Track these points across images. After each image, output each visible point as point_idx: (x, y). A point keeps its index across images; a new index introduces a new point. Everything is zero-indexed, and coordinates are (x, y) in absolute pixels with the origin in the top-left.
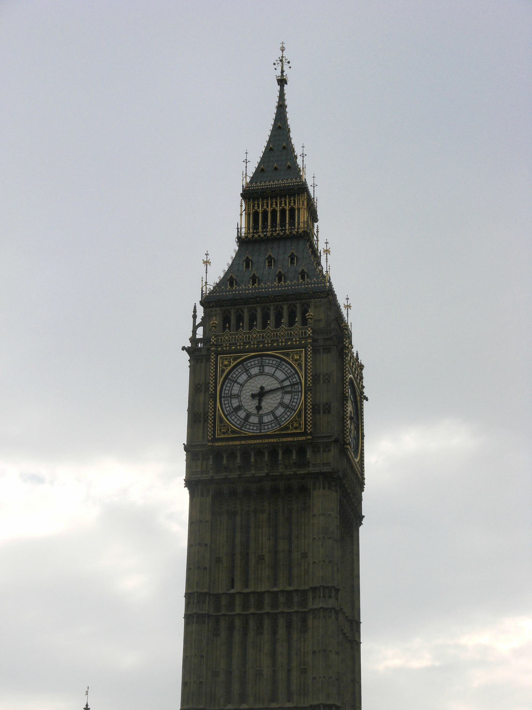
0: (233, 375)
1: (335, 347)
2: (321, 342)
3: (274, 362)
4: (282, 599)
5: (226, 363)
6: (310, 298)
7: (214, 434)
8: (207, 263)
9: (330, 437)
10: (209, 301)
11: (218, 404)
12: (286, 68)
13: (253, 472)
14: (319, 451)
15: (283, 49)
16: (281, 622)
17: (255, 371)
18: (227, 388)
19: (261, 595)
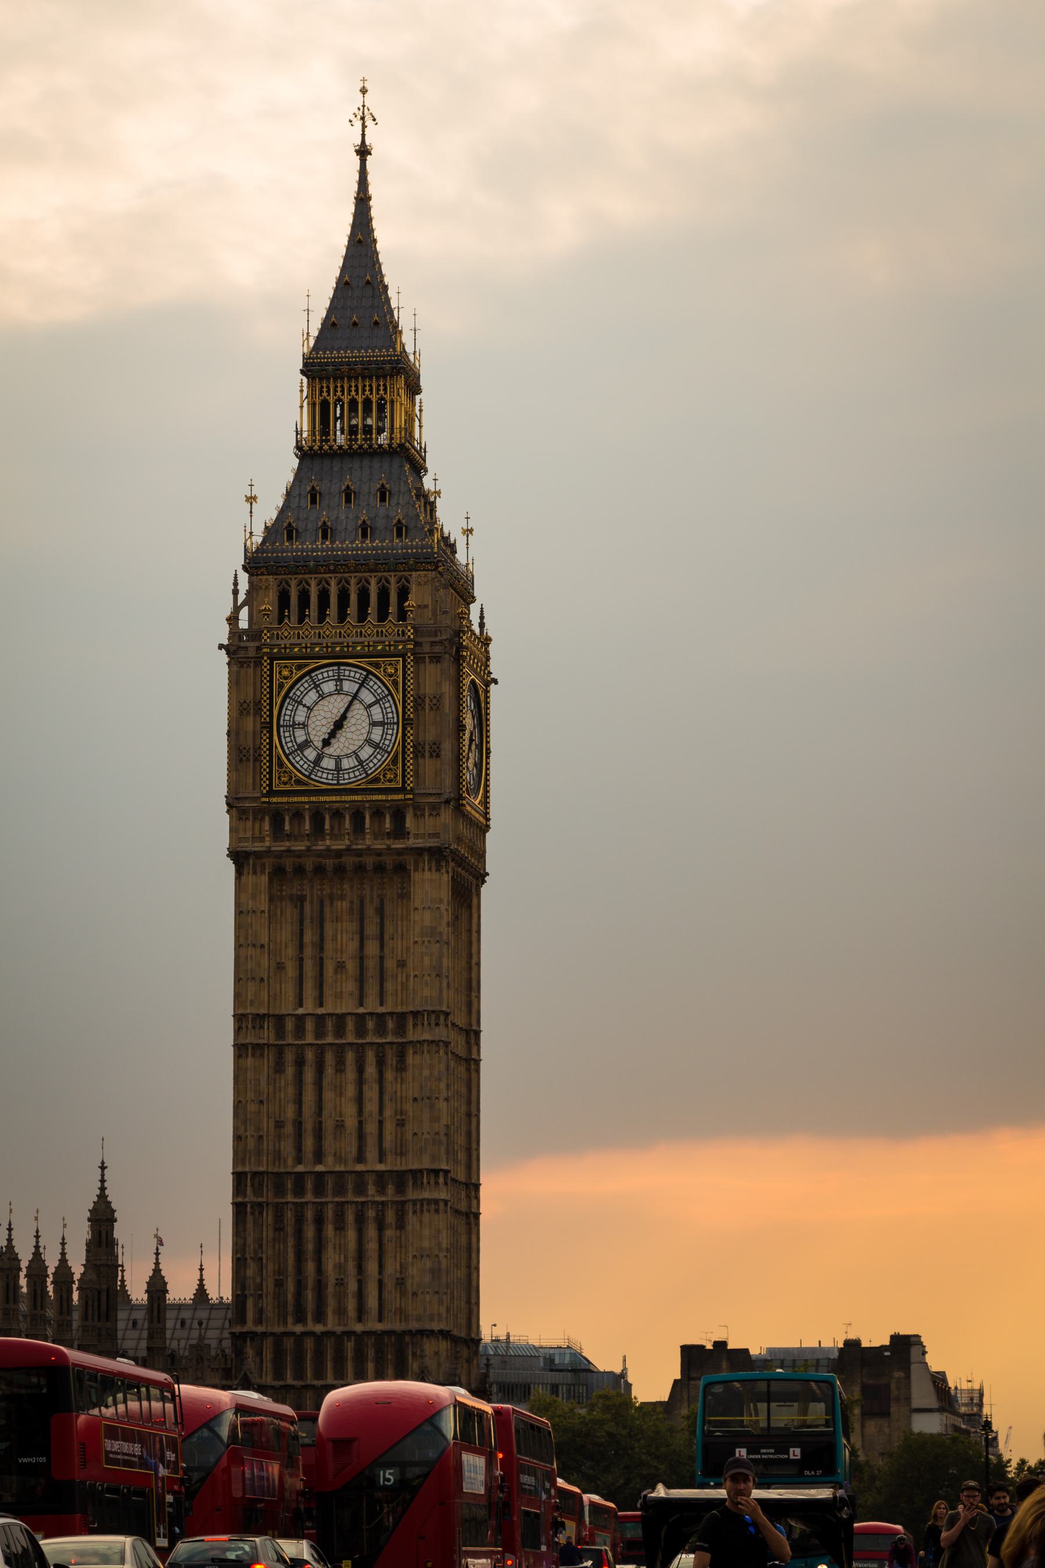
0: (296, 692)
1: (447, 656)
2: (426, 648)
3: (358, 675)
4: (370, 1024)
5: (286, 673)
6: (410, 570)
7: (270, 785)
8: (251, 499)
9: (440, 794)
10: (255, 564)
11: (276, 738)
12: (369, 122)
13: (328, 842)
14: (423, 815)
15: (364, 91)
16: (370, 1056)
17: (329, 687)
18: (288, 712)
19: (341, 1018)
